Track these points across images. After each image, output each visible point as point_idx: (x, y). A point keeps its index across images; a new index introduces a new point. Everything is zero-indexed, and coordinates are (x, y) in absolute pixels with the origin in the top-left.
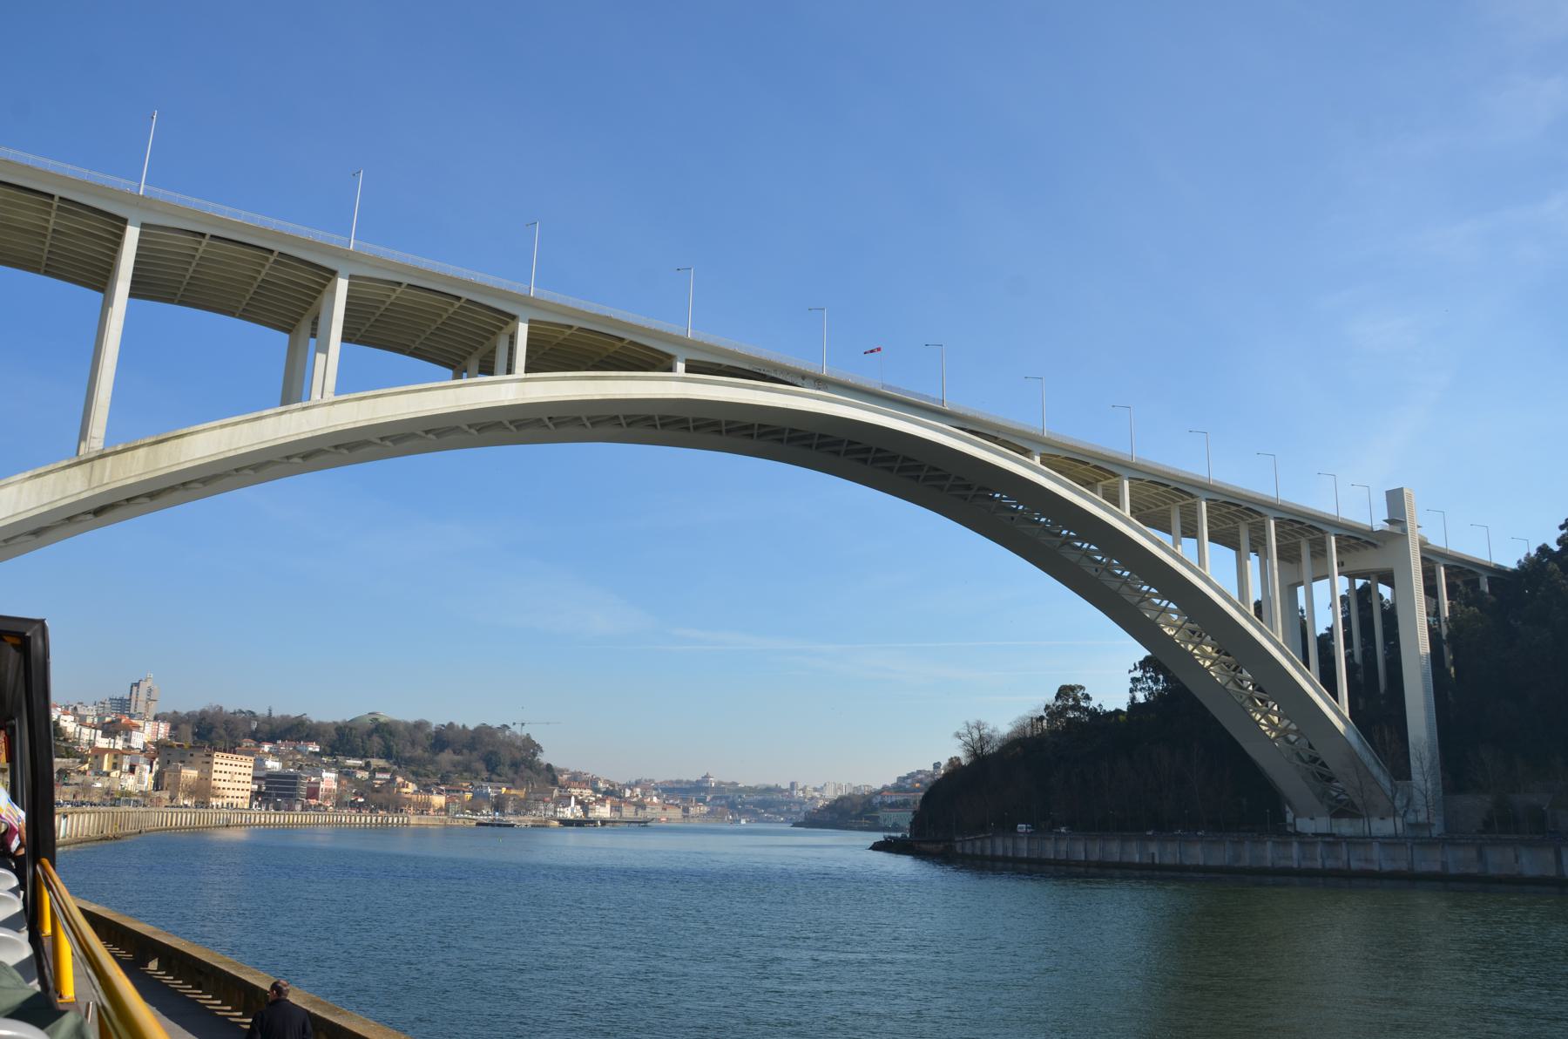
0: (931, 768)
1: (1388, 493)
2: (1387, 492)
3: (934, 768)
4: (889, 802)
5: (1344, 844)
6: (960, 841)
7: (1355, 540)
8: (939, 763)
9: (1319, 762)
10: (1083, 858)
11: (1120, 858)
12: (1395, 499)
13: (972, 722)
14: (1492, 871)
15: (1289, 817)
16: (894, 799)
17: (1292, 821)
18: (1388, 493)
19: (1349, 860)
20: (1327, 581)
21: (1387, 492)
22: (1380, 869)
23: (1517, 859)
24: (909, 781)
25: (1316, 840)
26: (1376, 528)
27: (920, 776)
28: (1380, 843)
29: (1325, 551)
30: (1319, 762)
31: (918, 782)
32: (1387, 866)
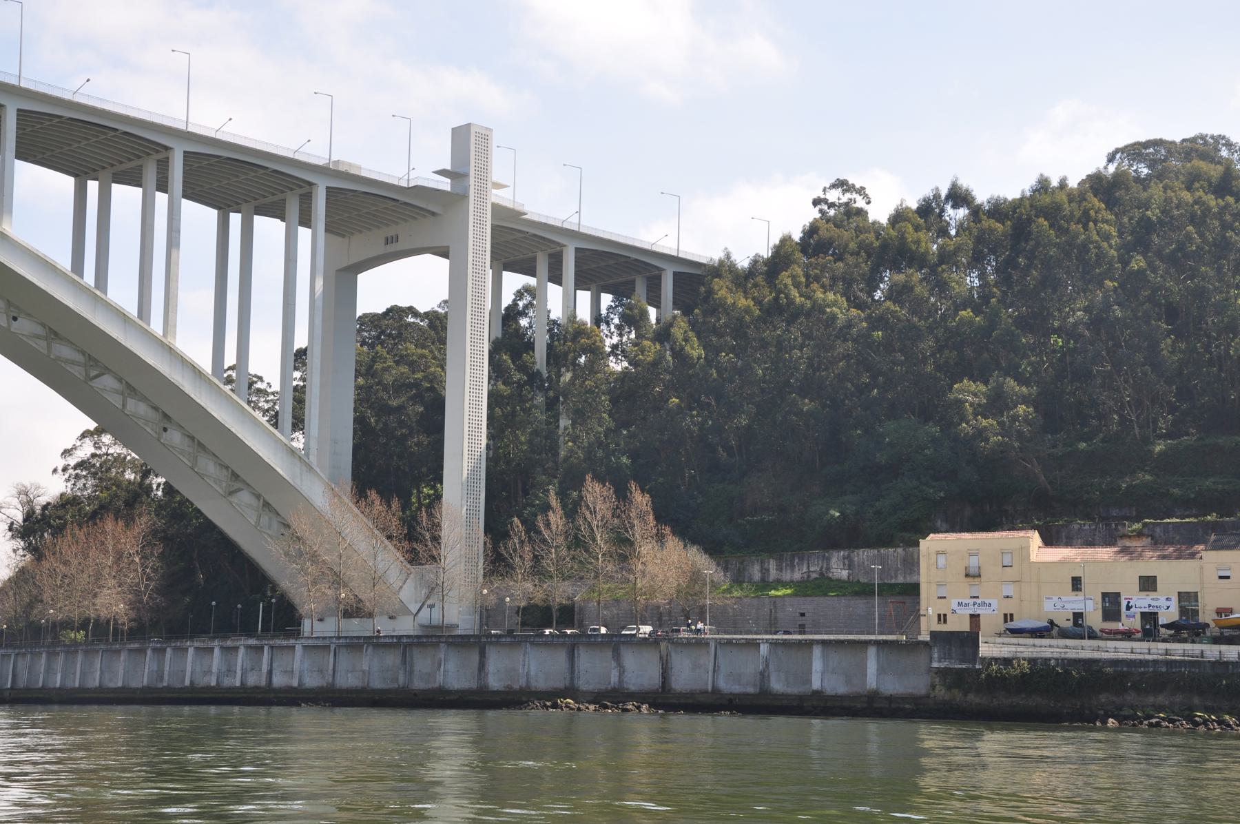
1: (455, 131)
18: (455, 131)
32: (312, 681)
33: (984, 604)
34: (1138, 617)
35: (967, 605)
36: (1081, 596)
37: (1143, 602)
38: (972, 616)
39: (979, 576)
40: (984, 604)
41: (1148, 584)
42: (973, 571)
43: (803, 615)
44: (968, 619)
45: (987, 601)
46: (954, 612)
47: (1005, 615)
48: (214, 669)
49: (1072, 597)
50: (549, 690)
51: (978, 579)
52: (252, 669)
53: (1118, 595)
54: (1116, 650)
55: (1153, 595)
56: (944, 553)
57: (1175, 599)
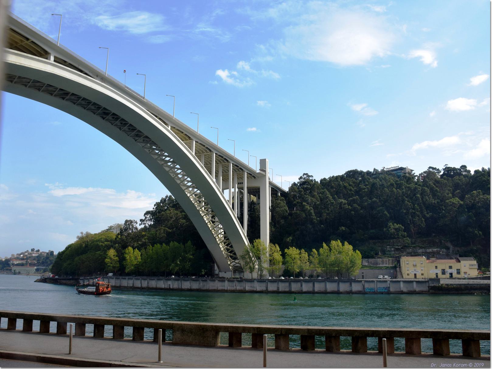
0: (30, 251)
1: (261, 160)
2: (260, 160)
3: (31, 251)
4: (16, 263)
5: (244, 281)
6: (82, 279)
7: (252, 175)
8: (34, 249)
9: (233, 252)
10: (140, 286)
11: (227, 288)
12: (263, 162)
13: (84, 232)
14: (293, 290)
15: (217, 272)
16: (18, 262)
17: (218, 273)
18: (261, 160)
19: (245, 287)
20: (228, 190)
21: (260, 160)
22: (256, 290)
23: (301, 286)
24: (22, 256)
25: (234, 280)
26: (257, 172)
27: (26, 254)
28: (257, 281)
29: (228, 179)
30: (233, 252)
31: (25, 256)
33: (417, 271)
34: (449, 274)
35: (413, 272)
36: (437, 270)
37: (450, 271)
38: (415, 274)
39: (416, 266)
40: (417, 271)
41: (451, 267)
42: (415, 265)
43: (363, 273)
44: (414, 275)
45: (418, 271)
46: (411, 273)
47: (422, 274)
48: (226, 286)
49: (436, 270)
50: (331, 291)
51: (415, 267)
52: (238, 286)
53: (444, 269)
54: (473, 282)
55: (452, 269)
56: (408, 261)
57: (456, 270)
